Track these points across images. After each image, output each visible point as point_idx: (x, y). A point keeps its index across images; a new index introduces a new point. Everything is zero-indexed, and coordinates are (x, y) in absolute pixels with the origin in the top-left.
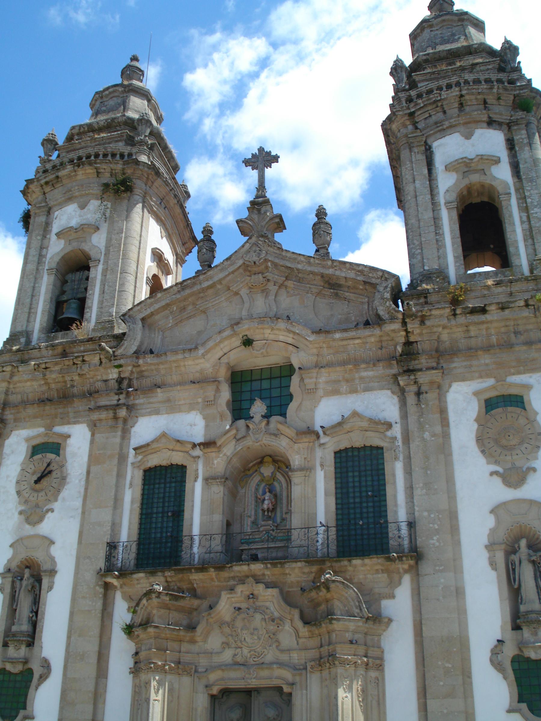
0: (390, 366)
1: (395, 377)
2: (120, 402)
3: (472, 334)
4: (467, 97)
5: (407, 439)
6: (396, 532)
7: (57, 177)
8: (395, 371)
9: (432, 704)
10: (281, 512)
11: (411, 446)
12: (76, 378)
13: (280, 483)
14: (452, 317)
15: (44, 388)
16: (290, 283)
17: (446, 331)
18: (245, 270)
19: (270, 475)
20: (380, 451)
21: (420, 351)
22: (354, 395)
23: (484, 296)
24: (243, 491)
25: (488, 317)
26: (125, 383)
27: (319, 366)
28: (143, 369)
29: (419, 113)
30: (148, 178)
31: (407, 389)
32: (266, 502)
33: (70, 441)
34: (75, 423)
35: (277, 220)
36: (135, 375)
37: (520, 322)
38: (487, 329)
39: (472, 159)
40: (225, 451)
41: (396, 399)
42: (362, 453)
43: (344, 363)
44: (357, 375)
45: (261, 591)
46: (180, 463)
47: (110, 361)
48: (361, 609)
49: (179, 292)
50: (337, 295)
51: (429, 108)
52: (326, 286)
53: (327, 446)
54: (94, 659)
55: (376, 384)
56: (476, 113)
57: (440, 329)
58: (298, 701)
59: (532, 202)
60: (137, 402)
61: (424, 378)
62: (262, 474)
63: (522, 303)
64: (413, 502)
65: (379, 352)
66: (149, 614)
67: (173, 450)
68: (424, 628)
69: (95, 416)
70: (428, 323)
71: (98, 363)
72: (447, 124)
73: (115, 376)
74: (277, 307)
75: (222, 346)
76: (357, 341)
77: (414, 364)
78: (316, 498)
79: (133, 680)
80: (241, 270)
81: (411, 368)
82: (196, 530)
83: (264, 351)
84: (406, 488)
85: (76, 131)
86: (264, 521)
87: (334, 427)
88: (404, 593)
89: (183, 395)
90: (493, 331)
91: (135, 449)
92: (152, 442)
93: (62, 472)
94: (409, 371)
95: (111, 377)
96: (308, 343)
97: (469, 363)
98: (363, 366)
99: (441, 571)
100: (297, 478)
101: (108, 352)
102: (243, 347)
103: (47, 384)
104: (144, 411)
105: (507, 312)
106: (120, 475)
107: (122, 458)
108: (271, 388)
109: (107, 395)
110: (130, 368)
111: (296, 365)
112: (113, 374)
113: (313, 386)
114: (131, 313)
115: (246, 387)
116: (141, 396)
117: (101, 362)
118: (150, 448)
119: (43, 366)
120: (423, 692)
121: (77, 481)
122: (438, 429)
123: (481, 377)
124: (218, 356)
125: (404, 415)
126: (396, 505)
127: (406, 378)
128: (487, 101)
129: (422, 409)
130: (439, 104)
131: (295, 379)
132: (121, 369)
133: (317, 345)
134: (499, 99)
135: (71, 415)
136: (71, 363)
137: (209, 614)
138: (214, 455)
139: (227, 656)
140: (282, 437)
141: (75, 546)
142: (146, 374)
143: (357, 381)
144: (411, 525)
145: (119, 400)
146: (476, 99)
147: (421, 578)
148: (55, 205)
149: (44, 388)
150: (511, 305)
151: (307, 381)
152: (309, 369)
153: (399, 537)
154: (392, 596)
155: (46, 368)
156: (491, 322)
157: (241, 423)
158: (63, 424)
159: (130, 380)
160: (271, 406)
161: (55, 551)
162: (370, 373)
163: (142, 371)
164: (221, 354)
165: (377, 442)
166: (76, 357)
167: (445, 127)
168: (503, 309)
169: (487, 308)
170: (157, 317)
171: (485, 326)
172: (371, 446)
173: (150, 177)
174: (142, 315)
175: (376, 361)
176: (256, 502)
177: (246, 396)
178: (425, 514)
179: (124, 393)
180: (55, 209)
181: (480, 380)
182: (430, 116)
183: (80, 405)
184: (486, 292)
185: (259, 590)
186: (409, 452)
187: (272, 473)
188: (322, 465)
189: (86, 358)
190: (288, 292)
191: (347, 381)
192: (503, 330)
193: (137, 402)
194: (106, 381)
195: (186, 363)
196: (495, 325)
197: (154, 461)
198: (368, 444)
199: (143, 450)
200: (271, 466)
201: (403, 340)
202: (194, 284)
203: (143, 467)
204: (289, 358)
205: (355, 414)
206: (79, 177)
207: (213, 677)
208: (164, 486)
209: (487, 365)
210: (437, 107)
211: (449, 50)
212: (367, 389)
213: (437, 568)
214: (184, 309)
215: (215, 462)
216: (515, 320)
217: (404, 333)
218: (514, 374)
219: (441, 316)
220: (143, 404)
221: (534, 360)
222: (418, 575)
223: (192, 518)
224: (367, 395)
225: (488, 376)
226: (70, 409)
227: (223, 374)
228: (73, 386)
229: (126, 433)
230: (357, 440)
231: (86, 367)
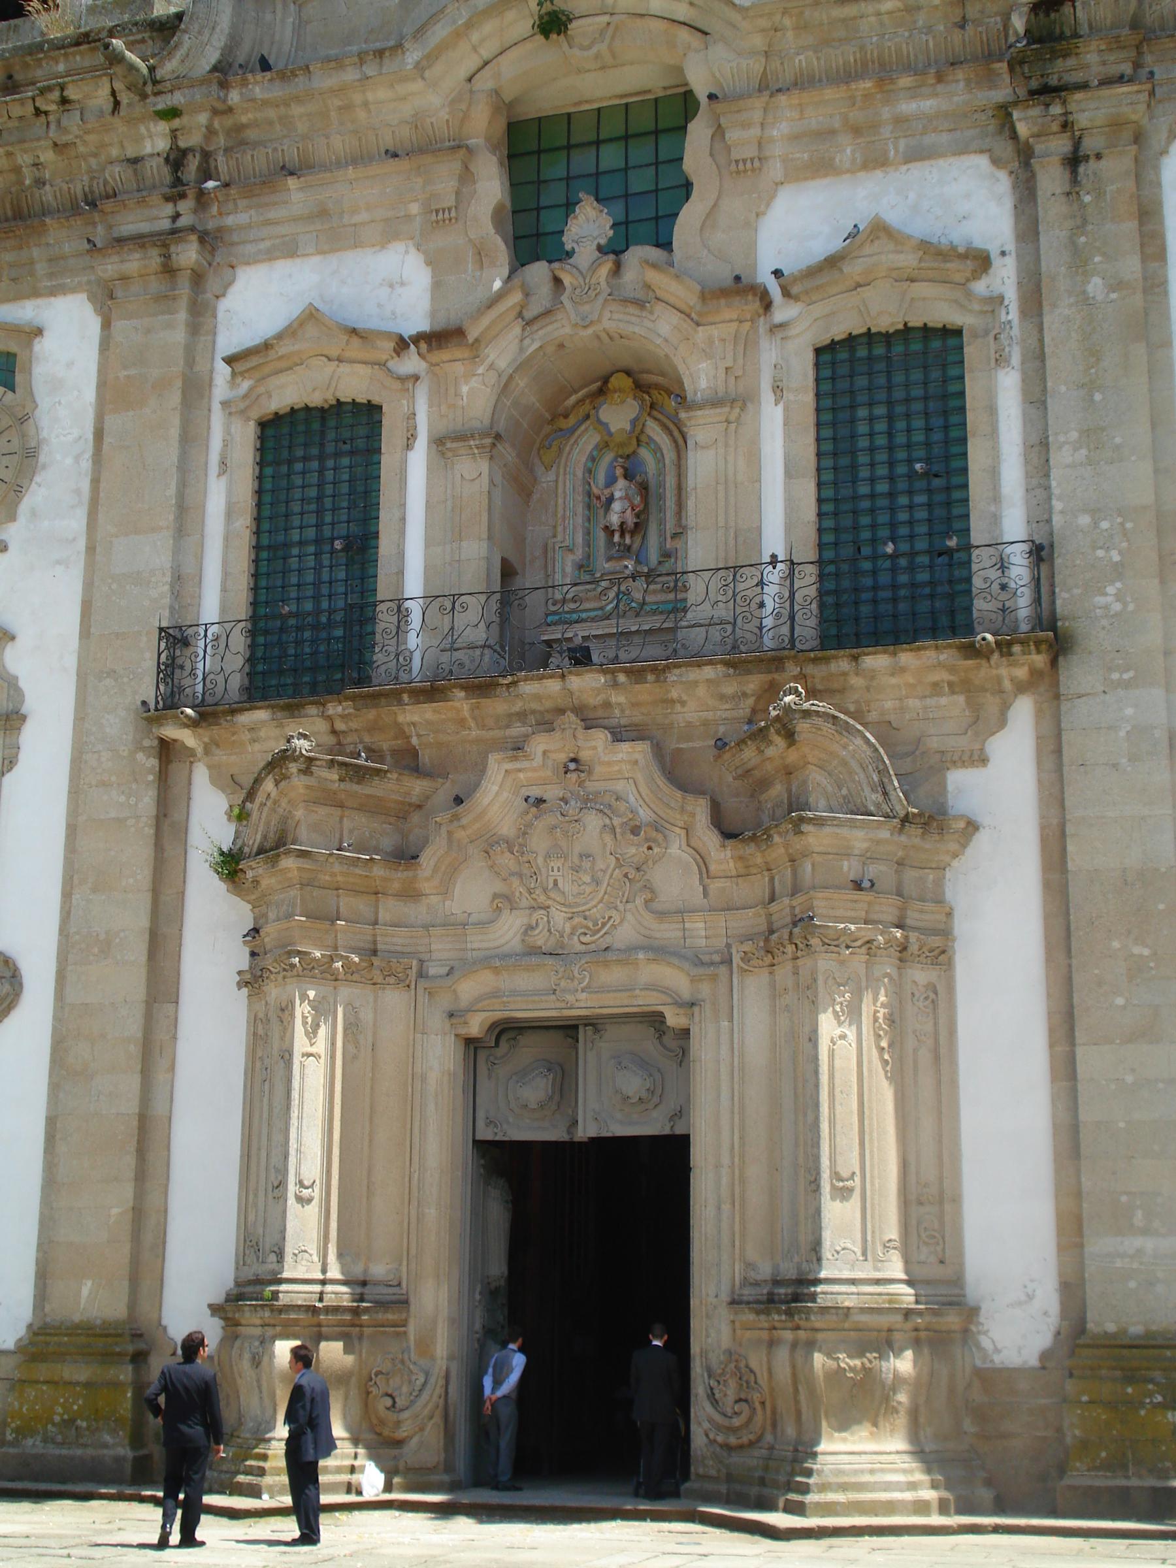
0: (989, 80)
1: (1004, 112)
2: (183, 222)
5: (1034, 298)
6: (994, 574)
8: (1002, 94)
9: (1089, 1060)
10: (662, 533)
11: (1047, 320)
12: (47, 156)
13: (657, 451)
19: (628, 427)
20: (952, 342)
21: (1084, 29)
22: (878, 173)
24: (551, 476)
27: (769, 87)
28: (244, 119)
31: (1039, 148)
32: (617, 506)
33: (44, 346)
34: (53, 292)
36: (221, 141)
40: (492, 357)
41: (1003, 182)
42: (898, 349)
43: (846, 76)
44: (886, 113)
45: (600, 749)
46: (362, 399)
47: (144, 96)
48: (885, 794)
53: (793, 332)
54: (138, 952)
55: (945, 138)
58: (707, 1050)
60: (230, 221)
61: (1090, 111)
62: (605, 425)
64: (1048, 488)
65: (957, 36)
66: (284, 820)
67: (340, 360)
68: (1070, 848)
69: (110, 267)
71: (110, 106)
73: (162, 144)
75: (475, 37)
77: (1061, 70)
78: (759, 485)
79: (250, 1004)
81: (1053, 81)
82: (414, 585)
83: (602, 47)
84: (1028, 447)
86: (609, 559)
87: (813, 272)
88: (1014, 749)
89: (363, 193)
91: (229, 360)
92: (280, 336)
93: (24, 436)
94: (1046, 92)
95: (148, 149)
96: (735, 16)
98: (905, 81)
99: (1127, 685)
100: (702, 428)
101: (132, 67)
102: (540, 38)
104: (250, 249)
106: (191, 438)
107: (195, 389)
108: (626, 169)
109: (142, 202)
110: (203, 118)
111: (701, 94)
112: (155, 140)
113: (750, 152)
115: (555, 168)
116: (242, 203)
117: (117, 104)
118: (272, 354)
120: (1065, 1025)
121: (69, 461)
122: (1131, 267)
124: (463, 72)
125: (1028, 229)
126: (996, 498)
127: (1036, 111)
129: (1083, 206)
131: (698, 132)
132: (176, 123)
133: (763, 23)
135: (41, 268)
136: (30, 109)
137: (456, 817)
138: (459, 368)
139: (508, 931)
140: (659, 308)
141: (74, 643)
142: (252, 134)
143: (886, 131)
144: (1041, 553)
145: (176, 217)
147: (1064, 707)
151: (732, 135)
152: (741, 97)
153: (1004, 587)
157: (539, 271)
158: (19, 297)
159: (206, 155)
160: (627, 223)
161: (18, 660)
162: (928, 105)
163: (240, 128)
164: (473, 63)
166: (42, 91)
172: (925, 328)
175: (941, 68)
176: (589, 507)
177: (554, 194)
178: (1084, 520)
179: (191, 193)
183: (64, 238)
185: (595, 748)
186: (1041, 340)
187: (634, 422)
188: (778, 389)
189: (72, 93)
191: (856, 131)
193: (230, 221)
194: (135, 161)
195: (370, 96)
197: (288, 392)
198: (916, 322)
199: (254, 361)
200: (630, 401)
203: (256, 413)
204: (679, 70)
205: (880, 229)
207: (469, 989)
208: (318, 466)
212: (918, 155)
213: (1115, 676)
215: (465, 389)
220: (249, 226)
222: (1057, 696)
223: (401, 555)
224: (918, 171)
226: (36, 252)
227: (481, 124)
228: (40, 183)
229: (201, 316)
230: (884, 311)
231: (72, 121)
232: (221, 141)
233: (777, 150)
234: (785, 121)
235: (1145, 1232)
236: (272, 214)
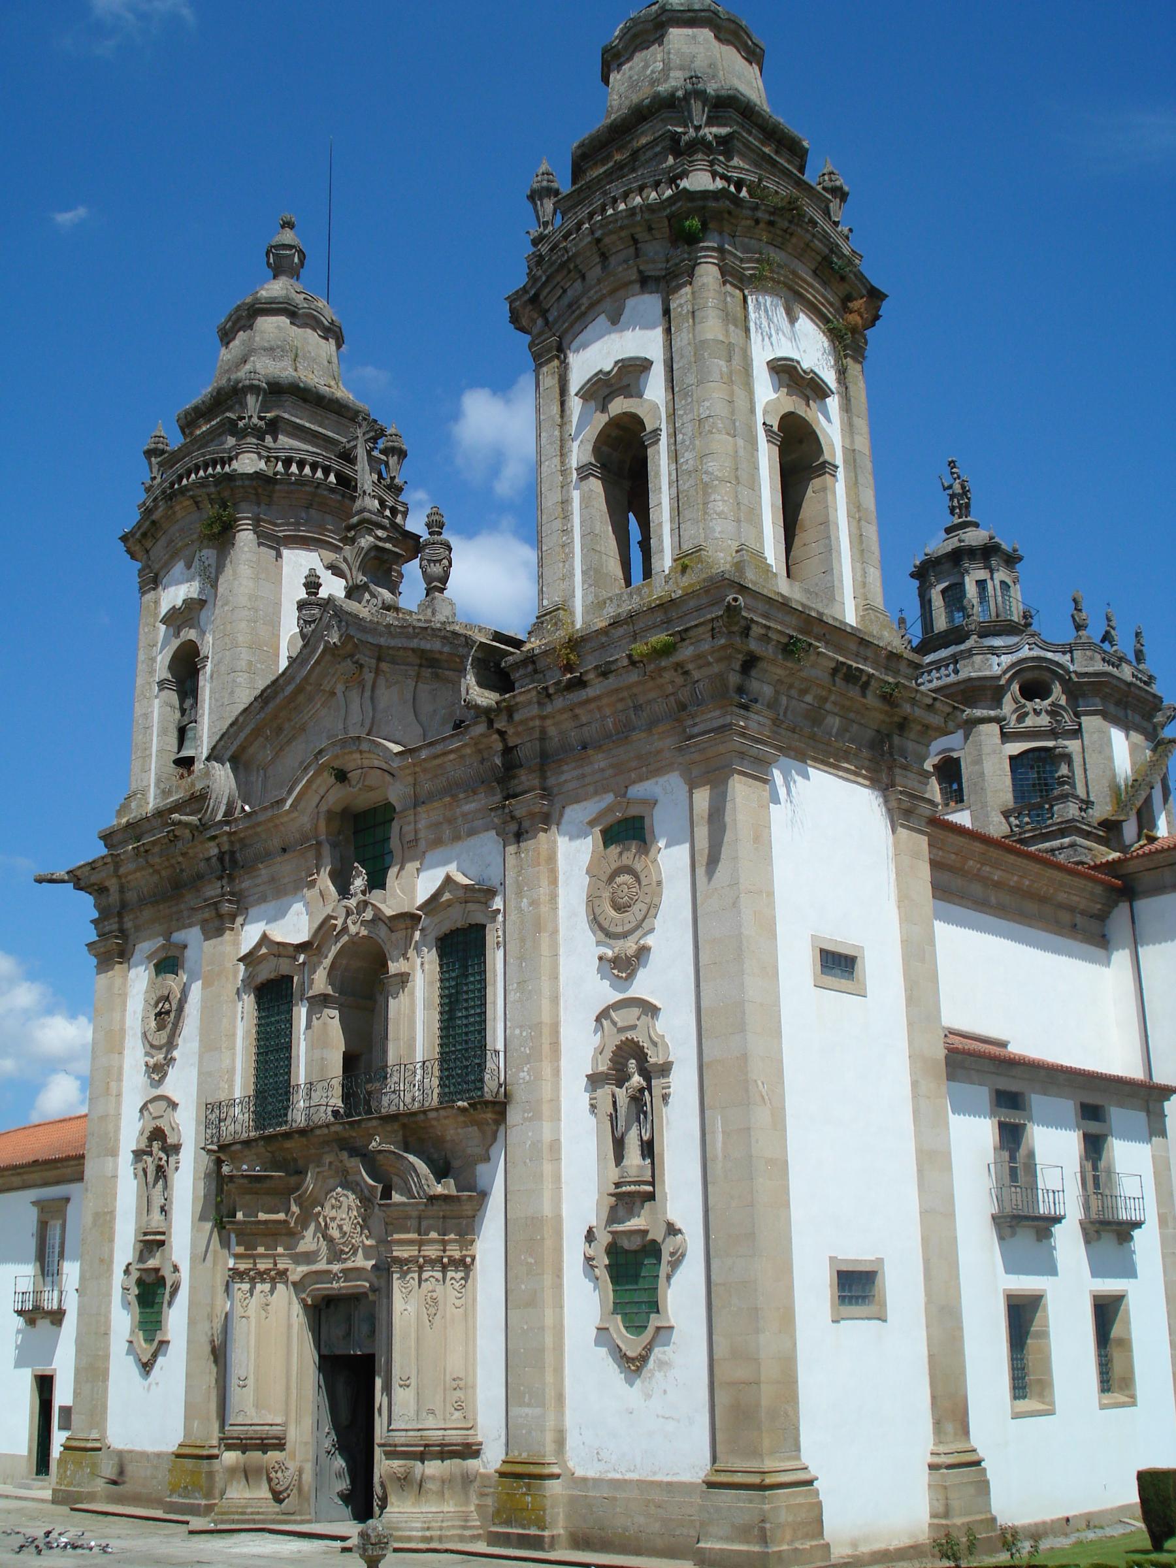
3: (584, 719)
4: (606, 240)
7: (154, 523)
12: (180, 859)
14: (546, 700)
15: (156, 878)
16: (384, 666)
17: (549, 722)
18: (333, 655)
23: (603, 646)
25: (590, 692)
26: (227, 858)
27: (417, 802)
28: (242, 835)
29: (545, 293)
30: (257, 494)
35: (373, 554)
37: (635, 690)
38: (599, 708)
39: (609, 373)
49: (262, 708)
50: (436, 676)
51: (559, 278)
52: (424, 662)
56: (620, 269)
57: (537, 723)
59: (684, 441)
63: (626, 662)
70: (517, 717)
72: (585, 302)
74: (374, 709)
75: (314, 787)
76: (452, 756)
80: (328, 657)
83: (360, 786)
85: (183, 421)
89: (285, 867)
90: (608, 711)
97: (580, 771)
99: (530, 1119)
103: (157, 872)
104: (251, 898)
105: (612, 678)
114: (216, 752)
119: (142, 849)
123: (596, 793)
124: (314, 804)
128: (637, 236)
129: (521, 859)
130: (572, 266)
133: (408, 771)
134: (650, 229)
135: (185, 913)
136: (167, 840)
143: (460, 821)
145: (223, 887)
146: (620, 238)
148: (161, 568)
149: (156, 878)
150: (613, 667)
154: (487, 1159)
155: (146, 851)
156: (597, 698)
164: (316, 799)
165: (479, 919)
167: (583, 308)
168: (605, 674)
169: (585, 678)
170: (251, 750)
171: (593, 705)
173: (260, 491)
174: (229, 753)
180: (162, 574)
181: (596, 799)
182: (565, 291)
184: (604, 639)
190: (387, 681)
192: (620, 706)
193: (243, 885)
194: (208, 859)
196: (605, 701)
201: (499, 746)
202: (276, 693)
203: (253, 985)
206: (179, 515)
209: (603, 770)
210: (570, 271)
211: (612, 124)
214: (280, 729)
216: (629, 687)
217: (496, 736)
218: (634, 782)
219: (530, 703)
221: (659, 752)
225: (606, 790)
228: (182, 870)
231: (180, 844)
232: (237, 846)
233: (422, 835)
234: (425, 818)
235: (529, 1405)
236: (259, 881)
